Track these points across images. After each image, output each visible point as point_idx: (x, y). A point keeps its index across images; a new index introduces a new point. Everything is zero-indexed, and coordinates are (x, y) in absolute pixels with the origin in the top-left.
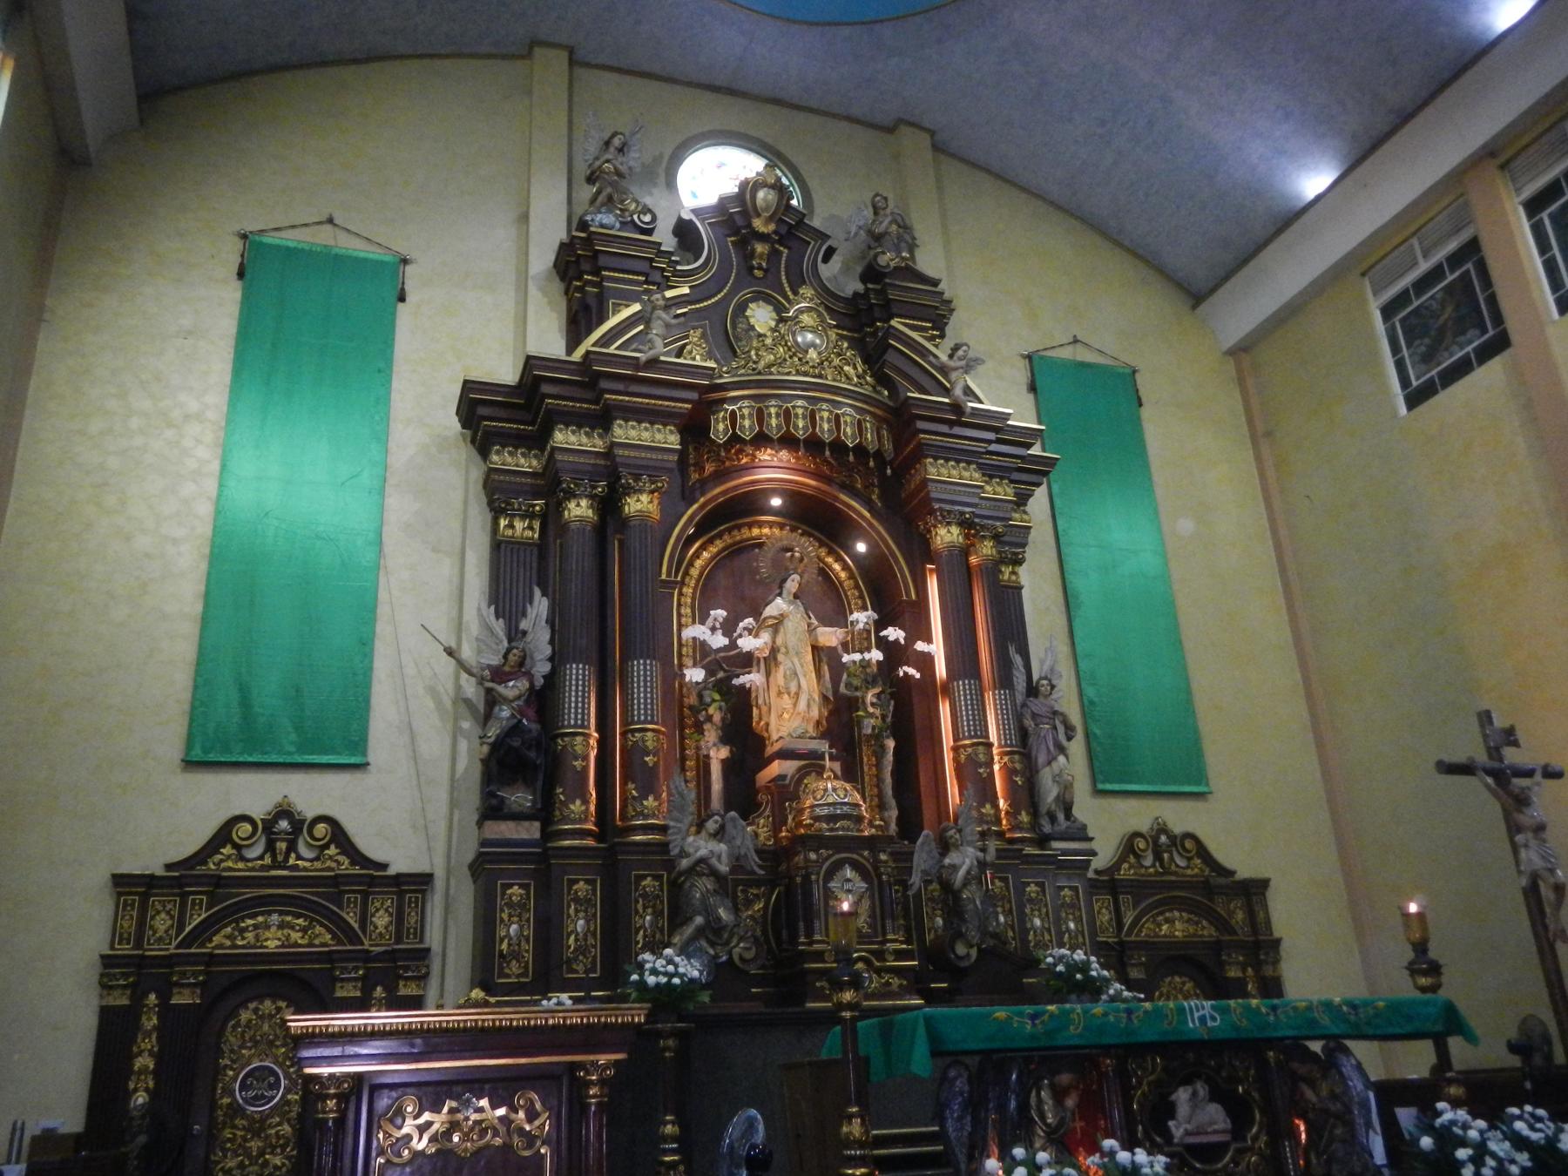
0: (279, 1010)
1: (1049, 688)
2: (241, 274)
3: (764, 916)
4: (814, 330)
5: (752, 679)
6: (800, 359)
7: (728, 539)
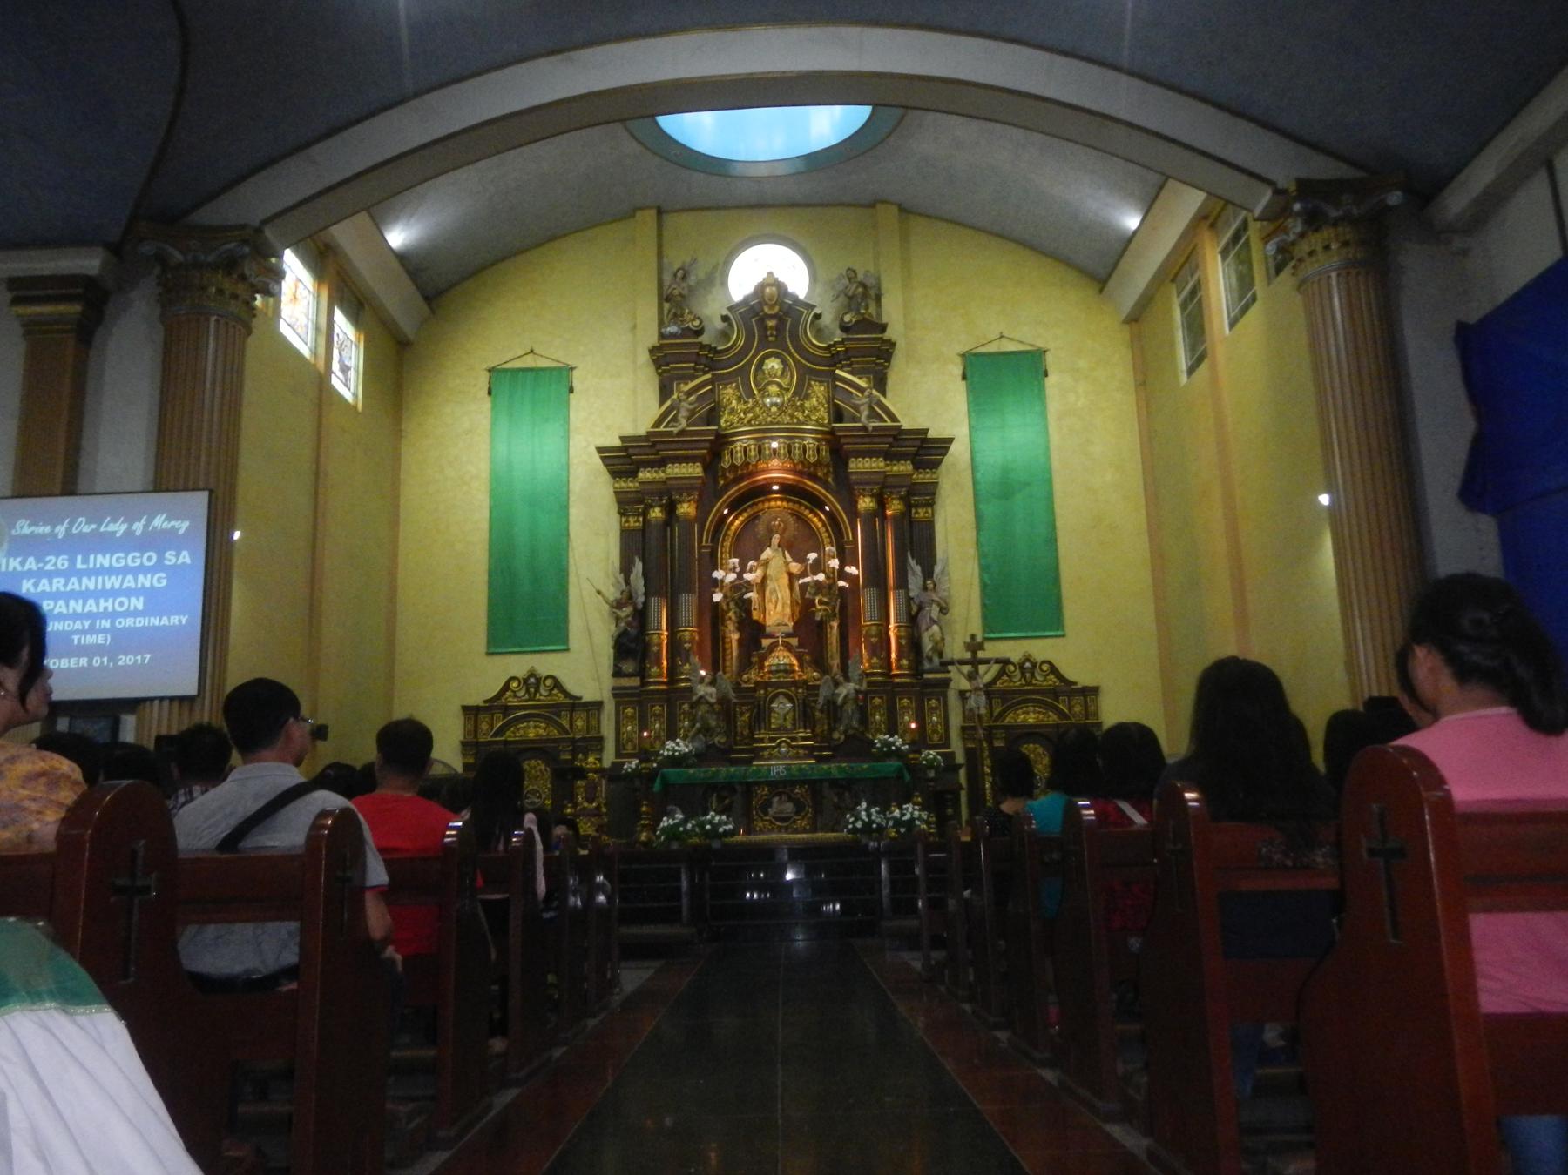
1: (932, 586)
2: (490, 393)
3: (750, 720)
4: (778, 396)
5: (752, 595)
6: (767, 414)
7: (750, 511)
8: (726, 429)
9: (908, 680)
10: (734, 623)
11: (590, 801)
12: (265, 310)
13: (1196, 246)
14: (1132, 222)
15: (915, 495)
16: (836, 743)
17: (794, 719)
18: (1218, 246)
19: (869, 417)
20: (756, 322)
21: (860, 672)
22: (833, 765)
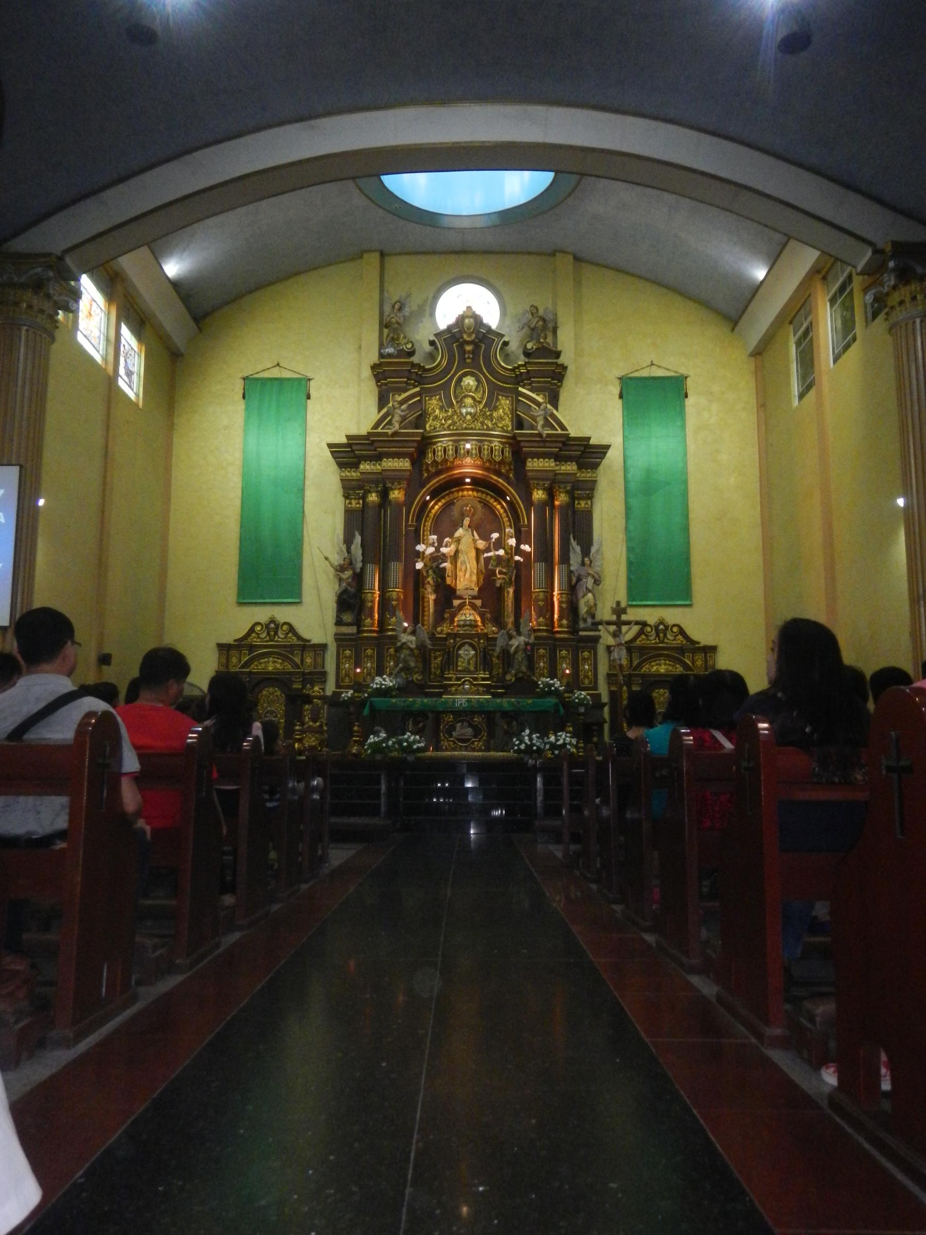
0: (276, 691)
1: (589, 562)
2: (244, 397)
3: (442, 663)
4: (472, 407)
5: (446, 565)
6: (463, 421)
8: (430, 432)
9: (566, 636)
10: (432, 587)
11: (315, 721)
12: (65, 323)
13: (809, 296)
14: (760, 273)
15: (578, 490)
16: (509, 683)
17: (476, 664)
18: (828, 295)
19: (543, 426)
20: (456, 346)
21: (529, 628)
22: (504, 700)
